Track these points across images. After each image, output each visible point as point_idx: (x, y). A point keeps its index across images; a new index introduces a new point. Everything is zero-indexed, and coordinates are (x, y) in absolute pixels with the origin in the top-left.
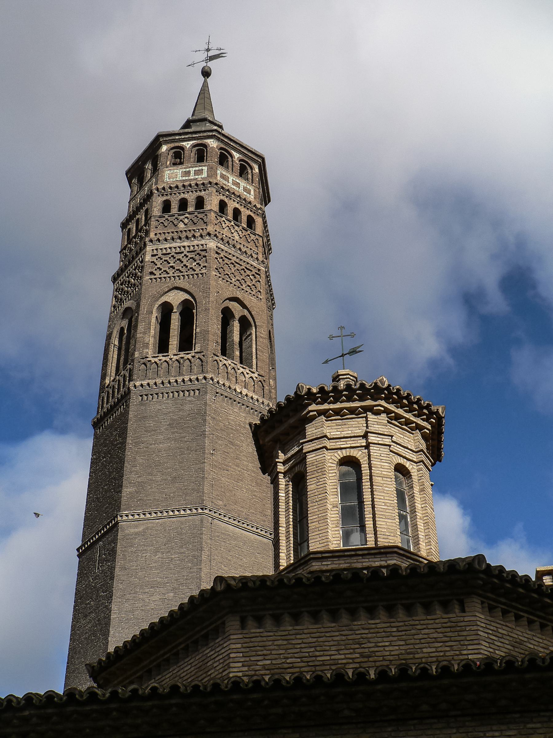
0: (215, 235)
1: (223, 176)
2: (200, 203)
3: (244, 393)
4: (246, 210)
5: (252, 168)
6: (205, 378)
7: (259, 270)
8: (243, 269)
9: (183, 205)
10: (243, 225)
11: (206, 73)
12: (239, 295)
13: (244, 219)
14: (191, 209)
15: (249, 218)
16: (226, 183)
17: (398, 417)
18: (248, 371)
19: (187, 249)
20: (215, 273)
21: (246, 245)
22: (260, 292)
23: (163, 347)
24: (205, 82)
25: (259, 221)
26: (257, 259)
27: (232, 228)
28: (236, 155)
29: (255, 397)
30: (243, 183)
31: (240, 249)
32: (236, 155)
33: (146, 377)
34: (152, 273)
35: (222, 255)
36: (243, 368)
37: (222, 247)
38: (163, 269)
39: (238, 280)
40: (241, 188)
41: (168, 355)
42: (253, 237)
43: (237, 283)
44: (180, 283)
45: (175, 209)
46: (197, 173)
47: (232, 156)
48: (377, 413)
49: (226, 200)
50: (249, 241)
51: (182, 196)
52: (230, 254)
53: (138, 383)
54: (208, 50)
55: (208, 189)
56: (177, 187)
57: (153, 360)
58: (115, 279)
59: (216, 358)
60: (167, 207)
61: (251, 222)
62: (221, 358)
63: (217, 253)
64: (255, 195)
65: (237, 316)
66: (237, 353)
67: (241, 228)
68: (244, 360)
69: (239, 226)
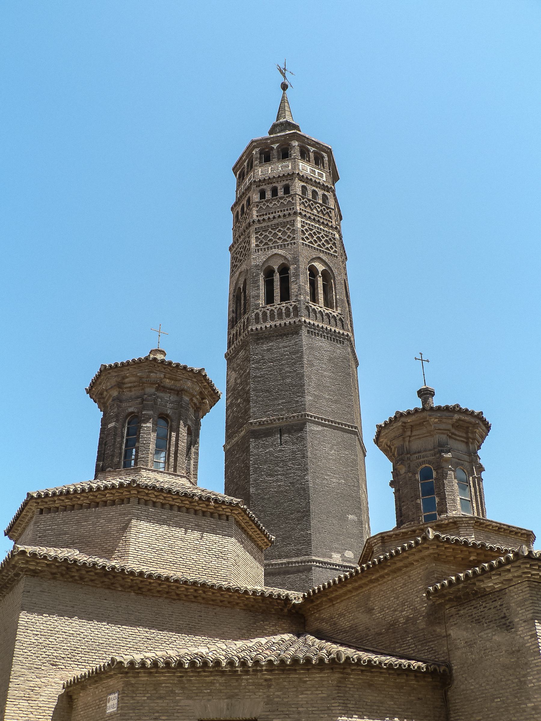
0: (300, 213)
2: (287, 189)
11: (284, 87)
13: (320, 196)
14: (281, 193)
15: (324, 195)
20: (302, 241)
23: (270, 299)
24: (284, 93)
35: (306, 227)
36: (327, 309)
40: (317, 174)
41: (274, 305)
45: (268, 195)
47: (308, 151)
51: (274, 185)
60: (263, 195)
62: (311, 304)
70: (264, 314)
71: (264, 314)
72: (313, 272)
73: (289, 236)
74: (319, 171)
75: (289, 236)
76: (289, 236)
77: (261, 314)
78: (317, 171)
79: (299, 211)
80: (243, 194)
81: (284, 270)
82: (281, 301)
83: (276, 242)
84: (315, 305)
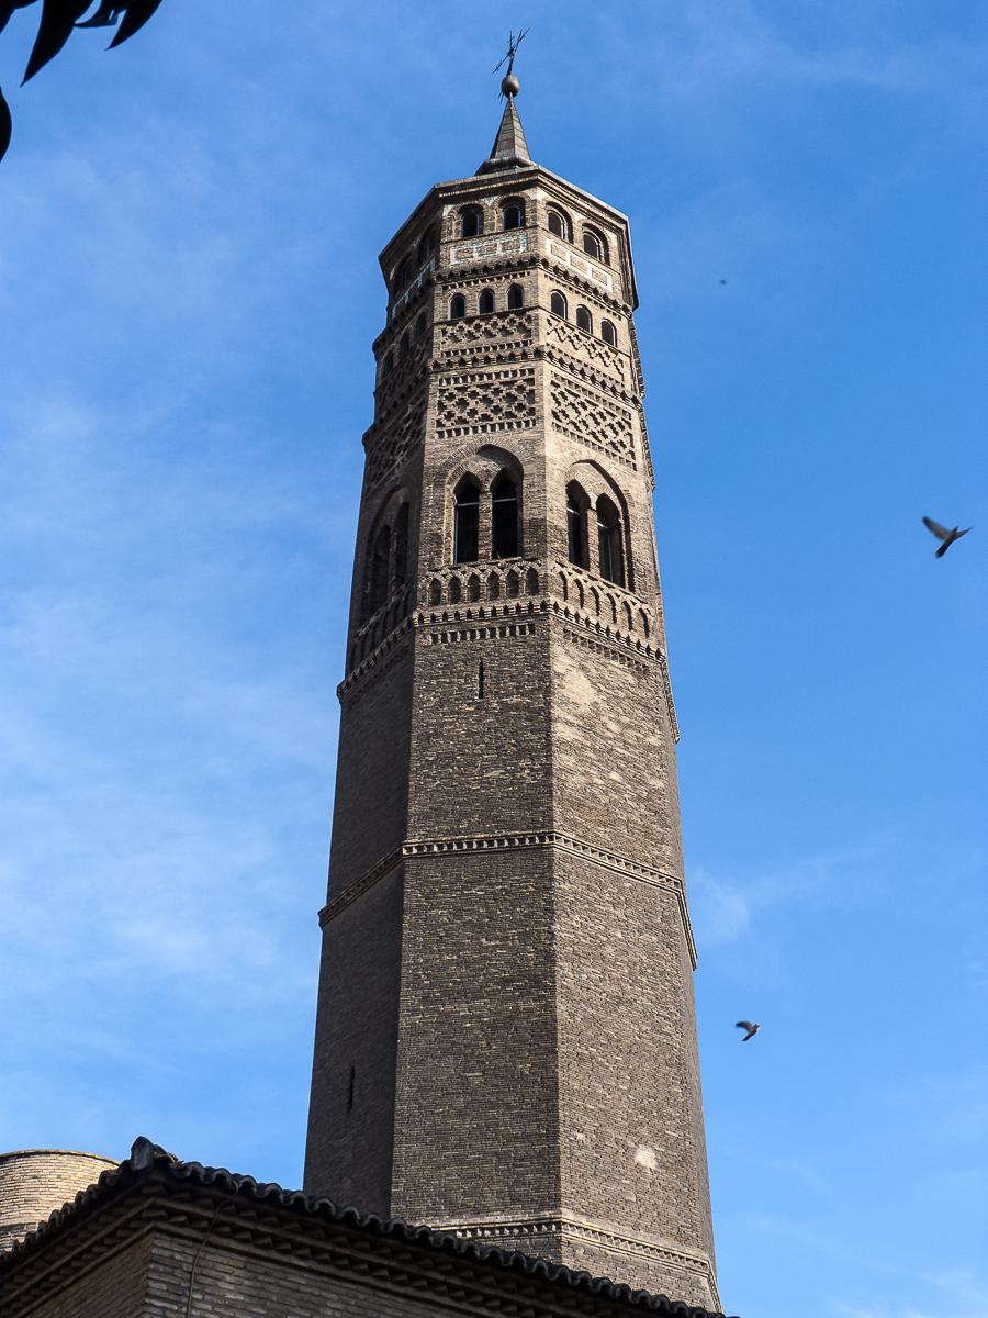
0: (550, 355)
6: (544, 606)
9: (487, 299)
18: (619, 593)
19: (503, 378)
23: (467, 552)
25: (621, 326)
26: (623, 395)
27: (574, 339)
32: (577, 217)
36: (610, 586)
38: (458, 415)
43: (590, 438)
45: (473, 308)
50: (608, 363)
51: (488, 284)
52: (577, 386)
55: (529, 274)
59: (564, 570)
60: (459, 304)
61: (608, 330)
67: (592, 340)
70: (455, 582)
71: (455, 582)
73: (520, 405)
74: (594, 267)
75: (520, 405)
76: (521, 407)
77: (445, 584)
78: (589, 267)
80: (408, 307)
82: (494, 557)
84: (580, 573)
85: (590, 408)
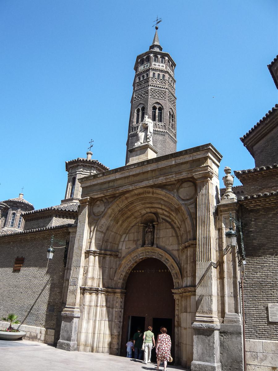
0: (150, 85)
1: (154, 65)
3: (158, 130)
4: (162, 73)
5: (165, 58)
7: (166, 91)
8: (160, 93)
10: (161, 78)
12: (158, 101)
16: (156, 66)
17: (86, 165)
21: (162, 84)
22: (165, 98)
23: (137, 122)
26: (165, 88)
28: (159, 56)
29: (162, 131)
30: (161, 65)
31: (159, 87)
33: (132, 131)
34: (135, 101)
37: (153, 88)
39: (158, 97)
40: (161, 66)
42: (164, 81)
43: (158, 98)
44: (141, 102)
46: (147, 66)
48: (80, 166)
49: (155, 72)
53: (131, 134)
54: (157, 20)
56: (141, 72)
57: (135, 126)
58: (131, 103)
63: (151, 90)
64: (166, 67)
65: (157, 108)
66: (157, 119)
68: (160, 120)
69: (159, 79)
72: (154, 108)
79: (150, 84)
81: (143, 109)
83: (138, 99)
85: (158, 92)
